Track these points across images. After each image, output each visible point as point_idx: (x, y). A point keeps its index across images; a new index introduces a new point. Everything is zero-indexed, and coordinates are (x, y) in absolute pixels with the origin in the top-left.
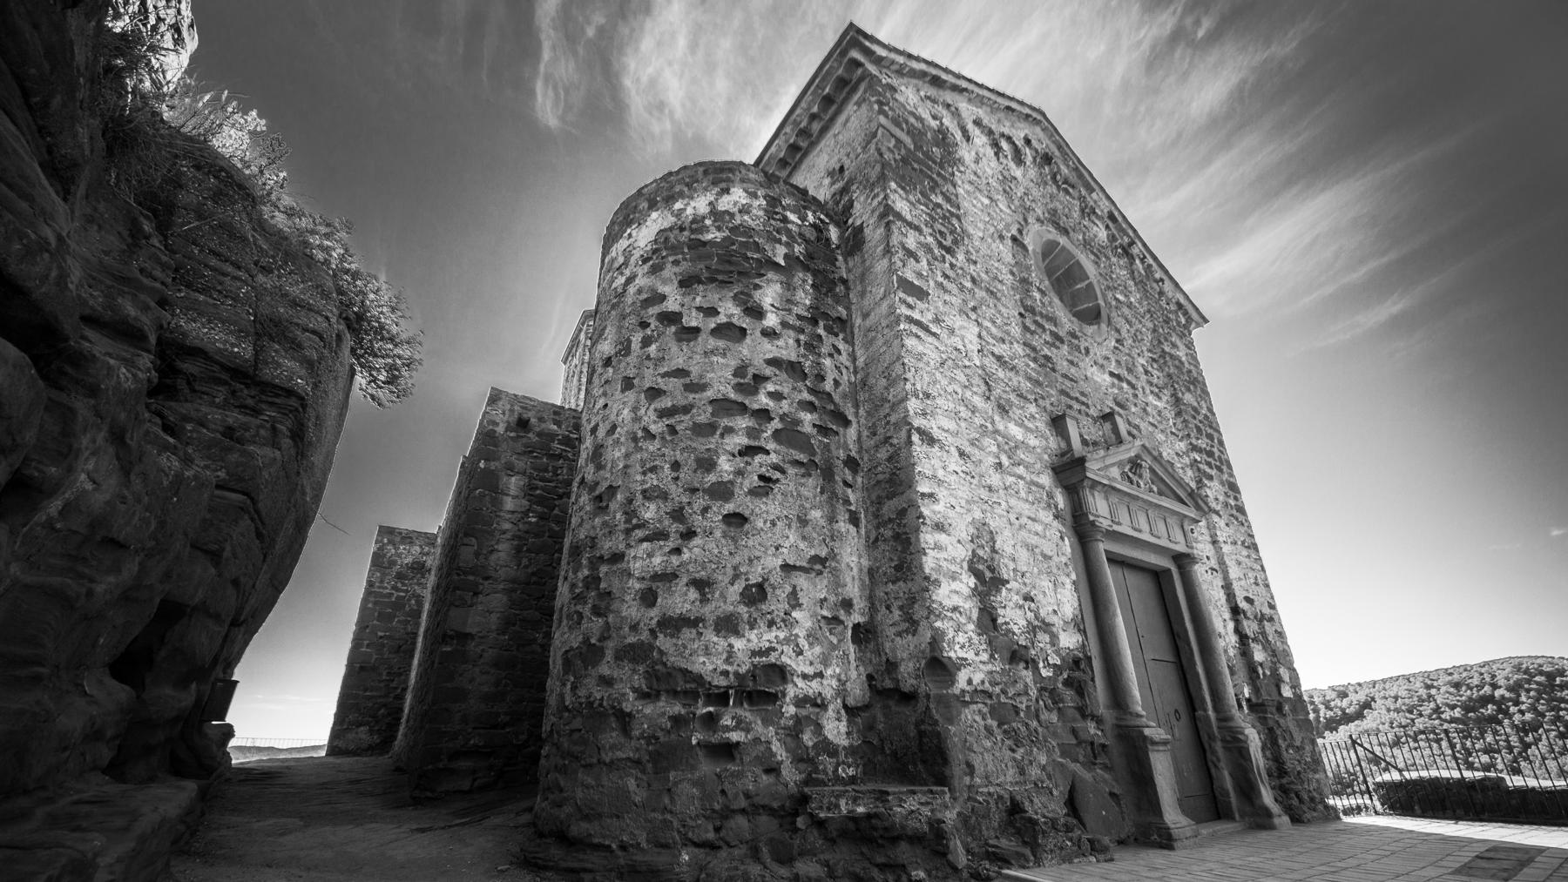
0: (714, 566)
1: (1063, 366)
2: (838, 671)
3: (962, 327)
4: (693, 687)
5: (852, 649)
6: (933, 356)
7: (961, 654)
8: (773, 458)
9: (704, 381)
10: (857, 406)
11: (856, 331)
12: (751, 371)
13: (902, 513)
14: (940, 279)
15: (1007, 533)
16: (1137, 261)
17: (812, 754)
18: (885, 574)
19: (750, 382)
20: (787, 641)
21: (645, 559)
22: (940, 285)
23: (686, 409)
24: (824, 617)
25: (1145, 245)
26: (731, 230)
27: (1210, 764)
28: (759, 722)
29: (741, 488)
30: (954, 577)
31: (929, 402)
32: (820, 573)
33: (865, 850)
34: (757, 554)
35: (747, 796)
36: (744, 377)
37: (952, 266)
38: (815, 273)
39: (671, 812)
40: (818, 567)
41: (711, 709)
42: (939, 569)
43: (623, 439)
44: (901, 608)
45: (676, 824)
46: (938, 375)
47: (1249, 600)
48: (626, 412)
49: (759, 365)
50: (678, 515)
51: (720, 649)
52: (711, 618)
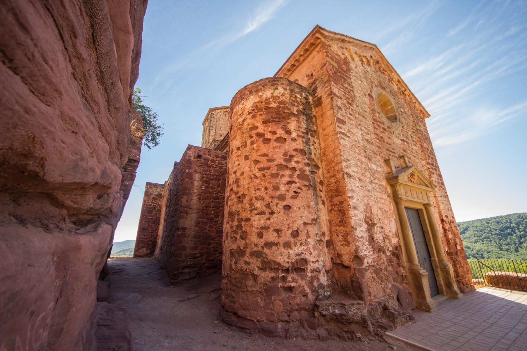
0: (281, 224)
1: (386, 140)
2: (323, 259)
3: (357, 132)
4: (276, 267)
5: (326, 249)
7: (365, 253)
8: (298, 185)
9: (273, 158)
10: (322, 162)
11: (320, 134)
12: (289, 154)
13: (342, 203)
14: (349, 116)
15: (375, 206)
16: (407, 96)
17: (317, 289)
18: (335, 223)
20: (307, 250)
21: (258, 221)
22: (349, 118)
23: (268, 168)
24: (317, 240)
25: (410, 90)
26: (279, 103)
27: (436, 276)
28: (300, 279)
29: (288, 196)
30: (361, 226)
31: (348, 162)
32: (315, 224)
33: (340, 325)
34: (295, 219)
35: (298, 305)
36: (286, 156)
37: (352, 110)
38: (306, 115)
39: (273, 310)
40: (314, 222)
41: (284, 274)
42: (356, 223)
43: (246, 178)
44: (343, 236)
45: (275, 314)
46: (350, 151)
47: (446, 216)
48: (247, 168)
50: (268, 206)
51: (286, 254)
52: (282, 243)
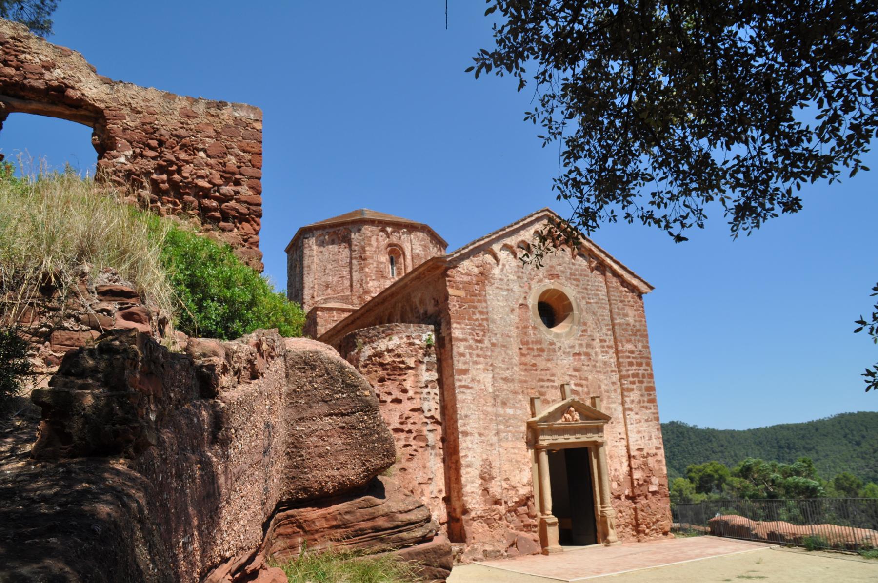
6: (469, 398)
8: (414, 447)
19: (404, 420)
30: (472, 482)
42: (467, 481)
46: (471, 406)
47: (639, 450)
49: (407, 413)
